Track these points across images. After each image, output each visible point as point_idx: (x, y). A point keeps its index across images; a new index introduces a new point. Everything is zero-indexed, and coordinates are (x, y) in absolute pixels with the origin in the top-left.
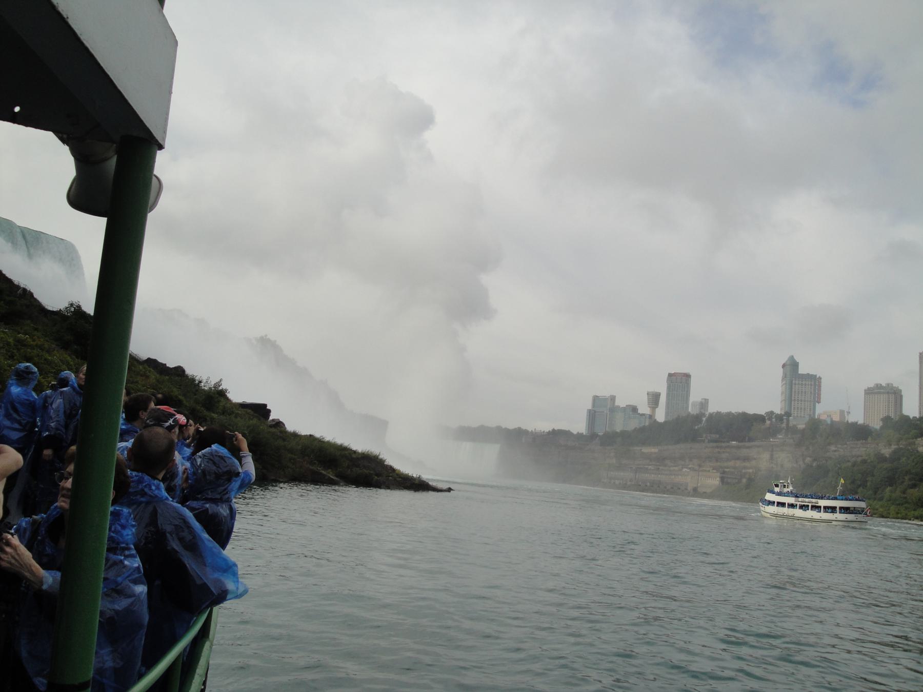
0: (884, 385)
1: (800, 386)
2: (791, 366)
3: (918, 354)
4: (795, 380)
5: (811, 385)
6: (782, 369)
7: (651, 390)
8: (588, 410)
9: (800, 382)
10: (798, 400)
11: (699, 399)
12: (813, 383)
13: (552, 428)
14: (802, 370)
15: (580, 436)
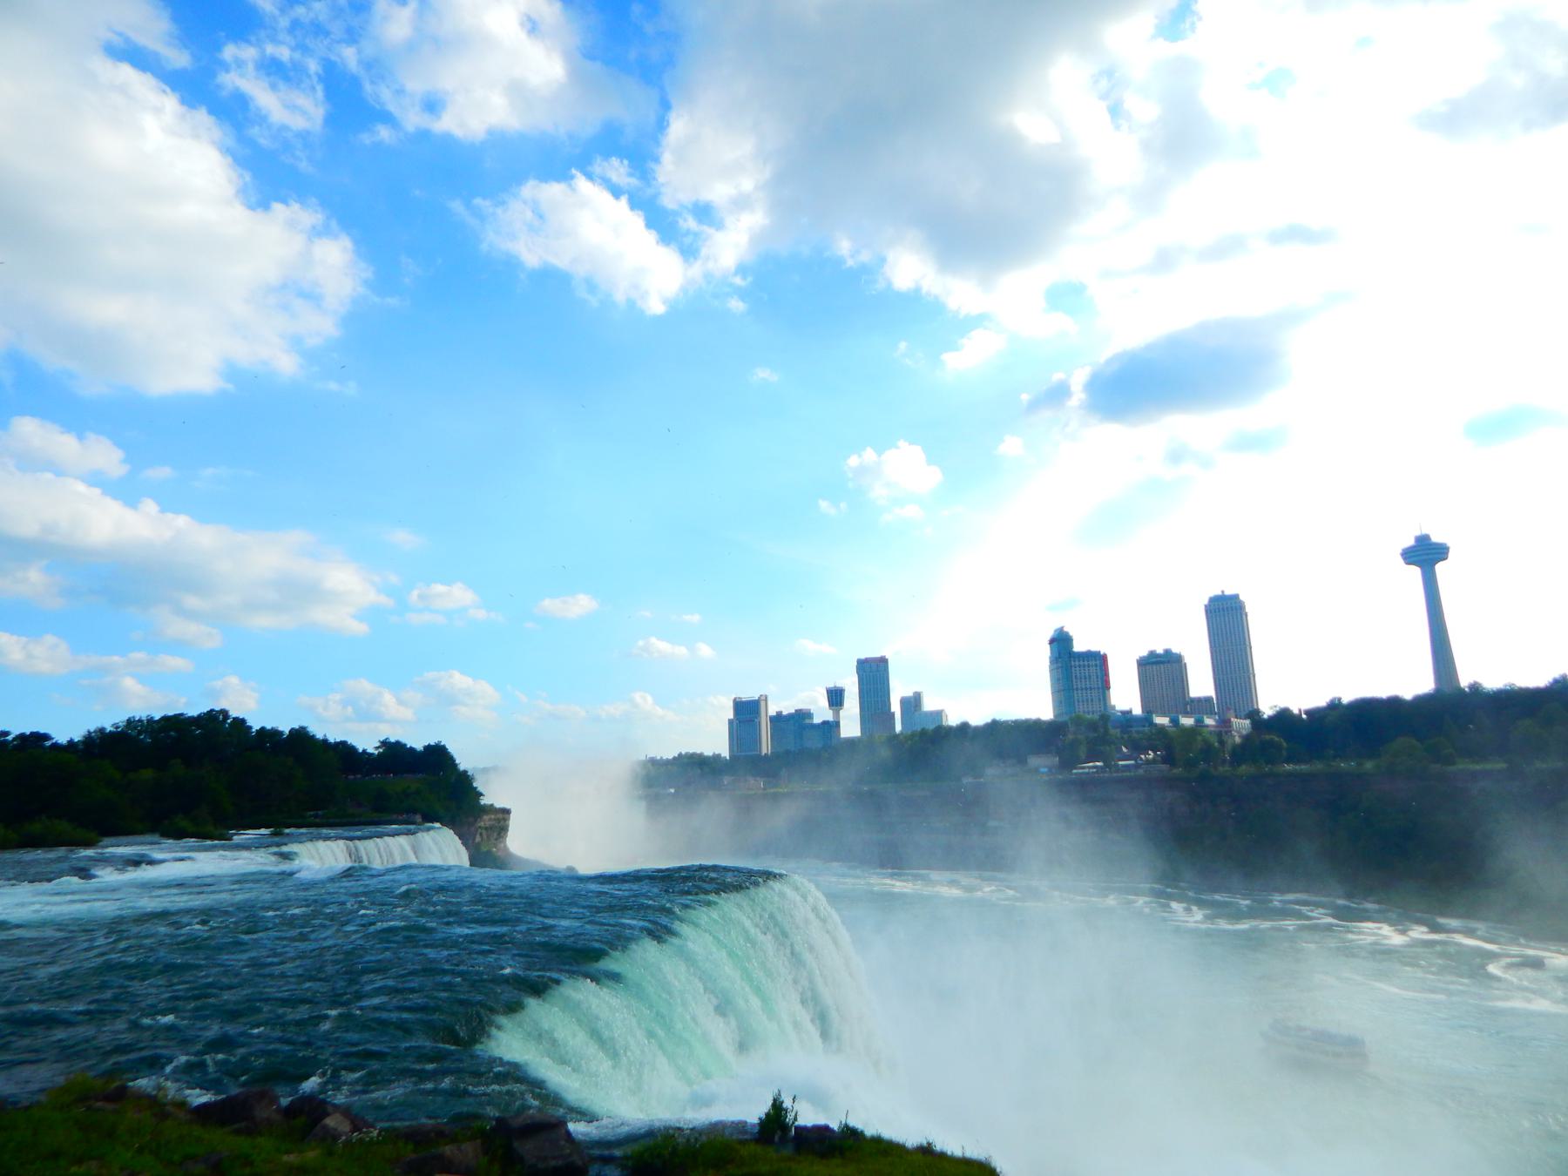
0: (1160, 651)
1: (1082, 668)
2: (1061, 642)
3: (1203, 607)
4: (1074, 661)
5: (1096, 665)
6: (1048, 646)
7: (831, 685)
8: (729, 720)
9: (1081, 663)
10: (1082, 689)
11: (909, 693)
12: (1098, 662)
13: (678, 752)
14: (1079, 646)
15: (717, 757)
